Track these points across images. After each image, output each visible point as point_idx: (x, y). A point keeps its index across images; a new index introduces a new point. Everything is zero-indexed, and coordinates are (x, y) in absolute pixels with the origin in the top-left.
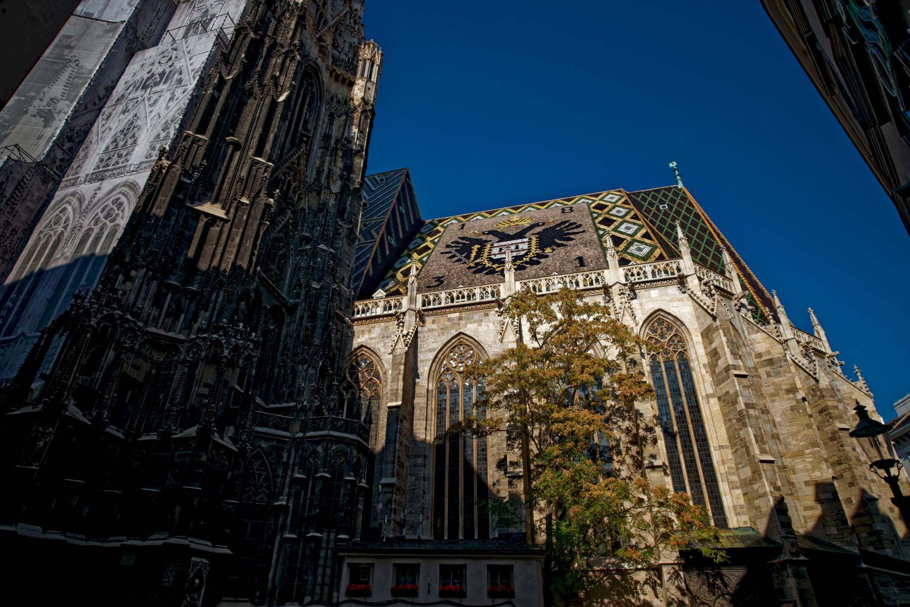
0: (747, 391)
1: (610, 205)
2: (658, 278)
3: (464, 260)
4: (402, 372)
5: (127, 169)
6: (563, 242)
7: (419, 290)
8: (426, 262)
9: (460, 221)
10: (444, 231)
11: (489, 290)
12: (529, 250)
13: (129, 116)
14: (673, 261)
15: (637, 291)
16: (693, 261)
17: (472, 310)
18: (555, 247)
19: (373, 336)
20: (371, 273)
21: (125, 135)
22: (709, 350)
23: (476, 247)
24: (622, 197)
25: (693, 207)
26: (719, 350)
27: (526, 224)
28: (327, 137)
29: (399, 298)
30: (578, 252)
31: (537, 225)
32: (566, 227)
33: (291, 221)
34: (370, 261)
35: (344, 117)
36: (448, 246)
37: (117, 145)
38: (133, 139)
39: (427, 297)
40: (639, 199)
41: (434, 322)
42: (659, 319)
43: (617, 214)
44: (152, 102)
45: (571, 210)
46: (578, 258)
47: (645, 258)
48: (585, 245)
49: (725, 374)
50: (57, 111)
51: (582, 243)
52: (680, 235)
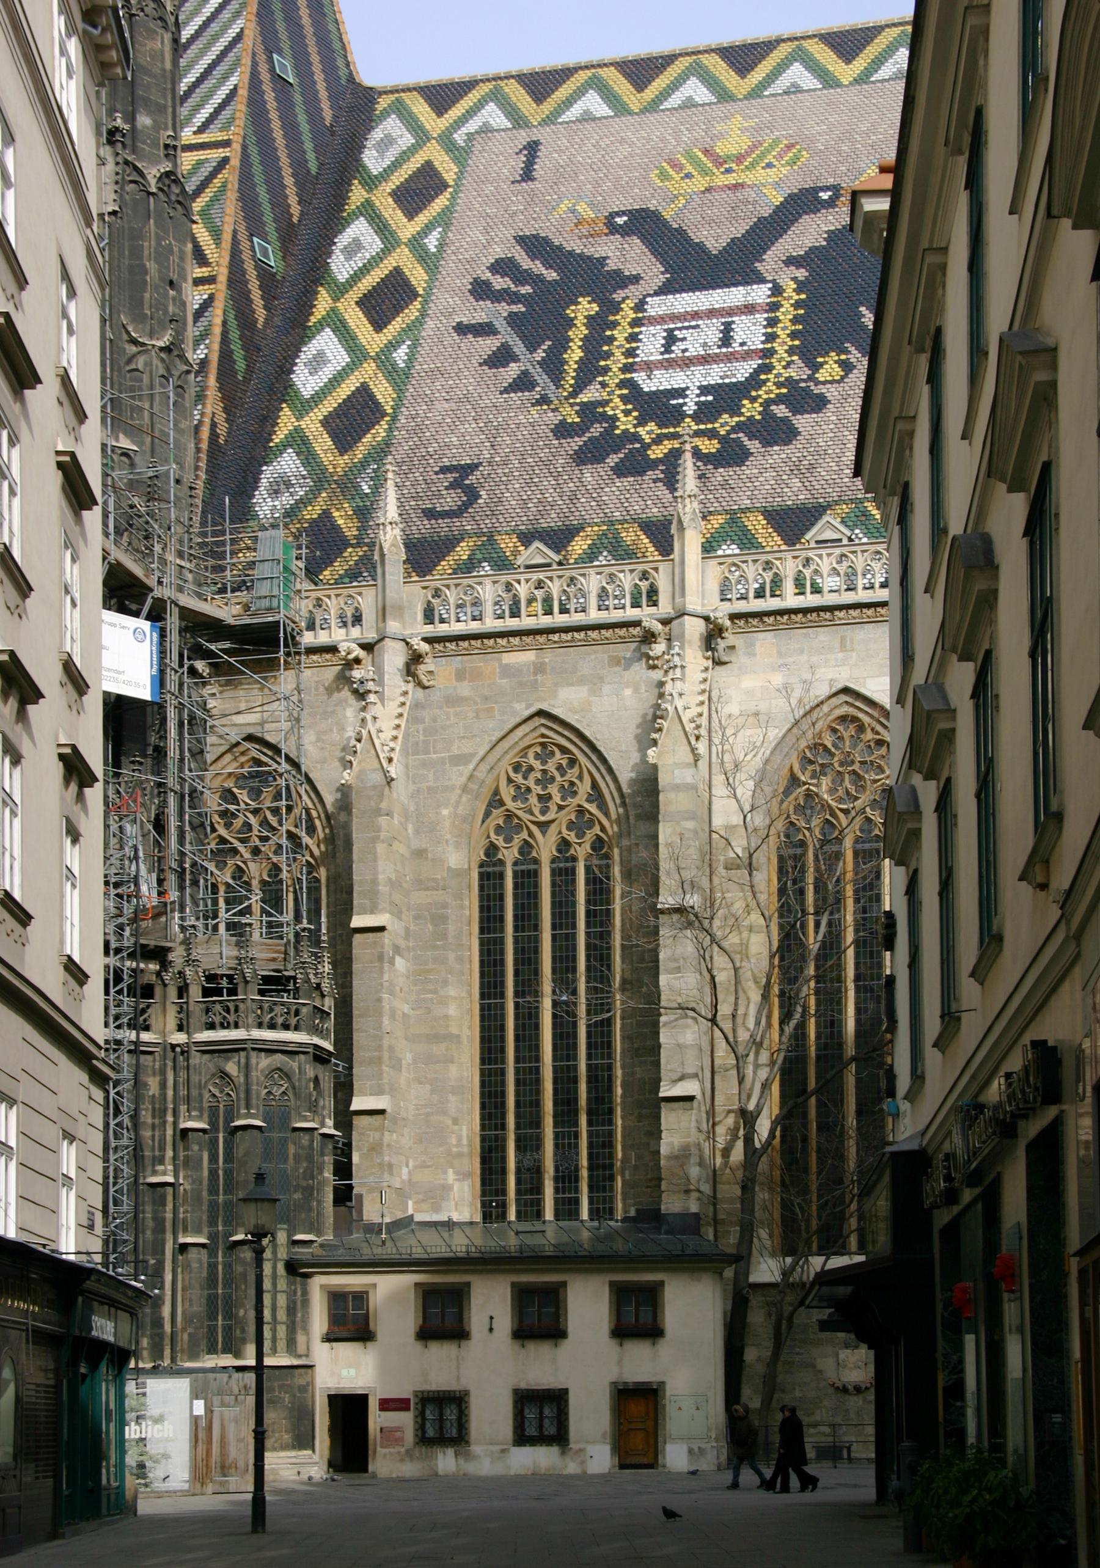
3: (541, 378)
8: (407, 374)
20: (222, 429)
23: (584, 308)
41: (460, 676)
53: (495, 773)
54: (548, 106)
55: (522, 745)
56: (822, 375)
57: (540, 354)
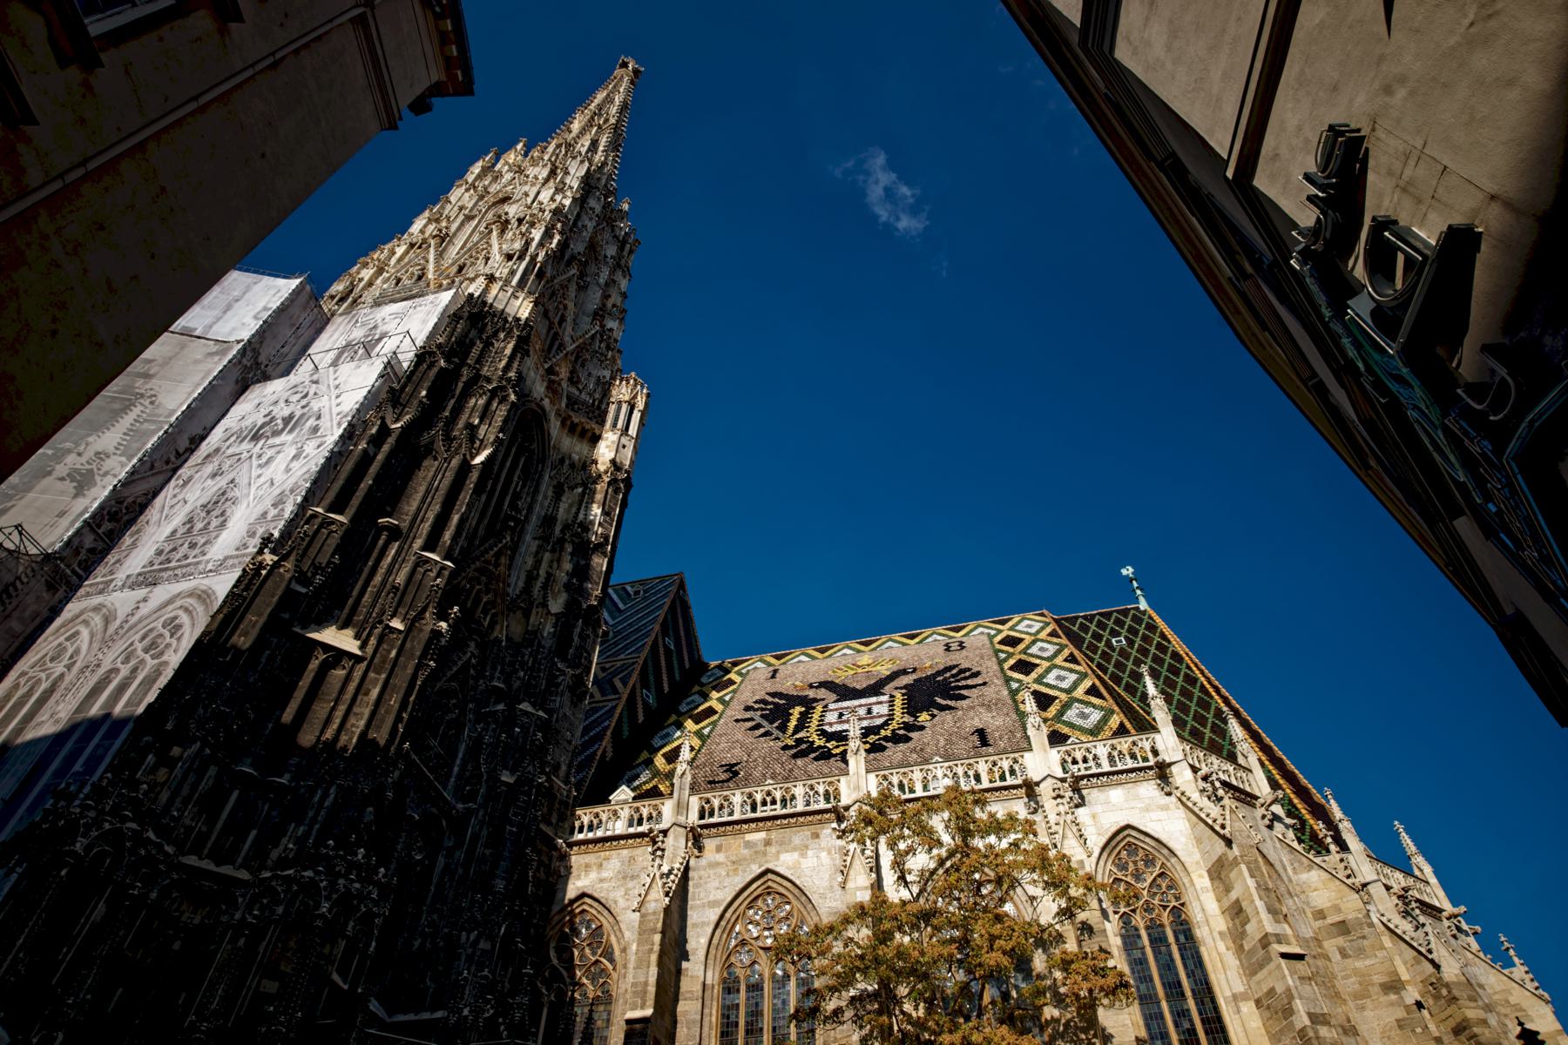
0: (1308, 988)
1: (1028, 639)
2: (1120, 767)
3: (776, 733)
4: (657, 948)
5: (201, 567)
6: (949, 703)
7: (694, 789)
8: (708, 736)
9: (769, 665)
10: (742, 682)
11: (821, 789)
12: (891, 717)
13: (222, 482)
14: (1144, 737)
15: (1084, 792)
16: (1179, 736)
17: (788, 826)
18: (935, 712)
19: (605, 874)
20: (610, 754)
21: (208, 512)
22: (1227, 903)
23: (797, 711)
24: (1047, 624)
25: (1169, 642)
26: (1244, 904)
27: (885, 670)
28: (549, 521)
29: (658, 802)
30: (976, 719)
31: (904, 672)
32: (953, 676)
33: (473, 661)
34: (609, 733)
35: (580, 490)
36: (747, 709)
37: (192, 527)
38: (221, 519)
39: (708, 801)
40: (1075, 629)
41: (719, 849)
42: (1129, 844)
43: (1039, 653)
44: (264, 460)
45: (961, 646)
46: (977, 731)
47: (1094, 732)
48: (989, 708)
49: (1262, 952)
50: (101, 472)
51: (983, 705)
52: (1151, 690)
53: (737, 913)
54: (782, 661)
55: (755, 894)
56: (920, 719)
57: (776, 724)
